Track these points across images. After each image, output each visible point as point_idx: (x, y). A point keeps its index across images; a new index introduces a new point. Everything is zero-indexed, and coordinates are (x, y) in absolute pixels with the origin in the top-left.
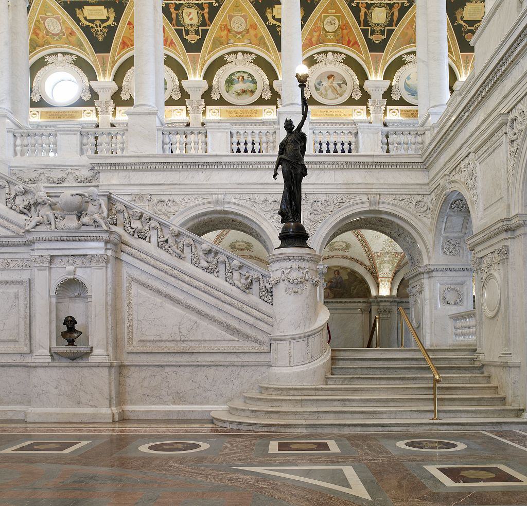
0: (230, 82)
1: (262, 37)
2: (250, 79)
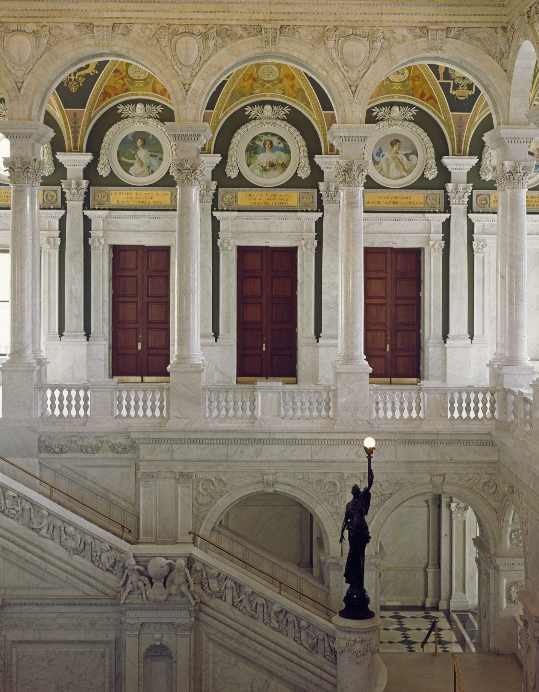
0: (252, 150)
1: (301, 90)
2: (281, 145)
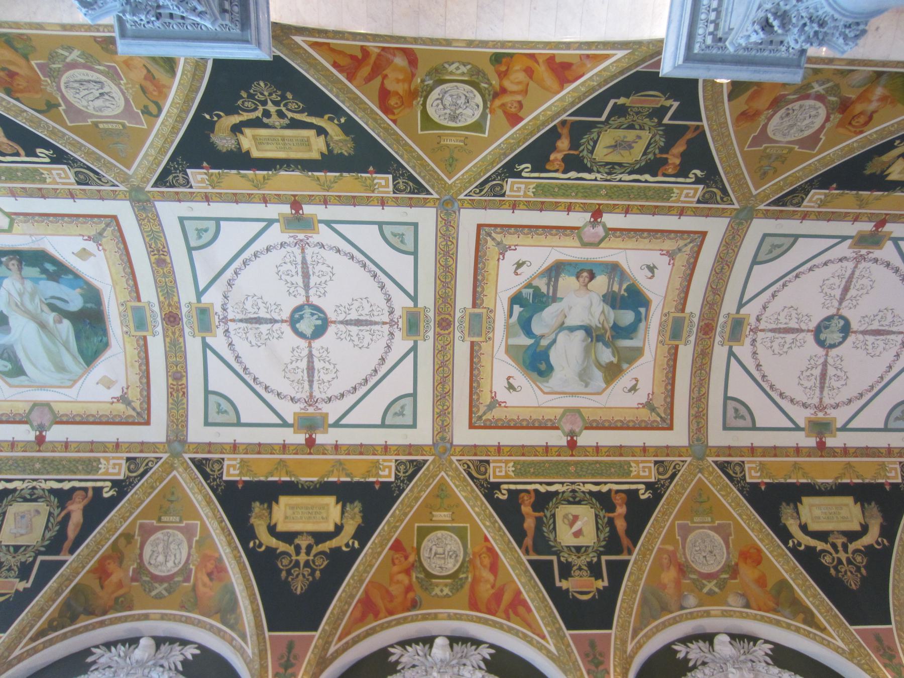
1: (783, 585)
